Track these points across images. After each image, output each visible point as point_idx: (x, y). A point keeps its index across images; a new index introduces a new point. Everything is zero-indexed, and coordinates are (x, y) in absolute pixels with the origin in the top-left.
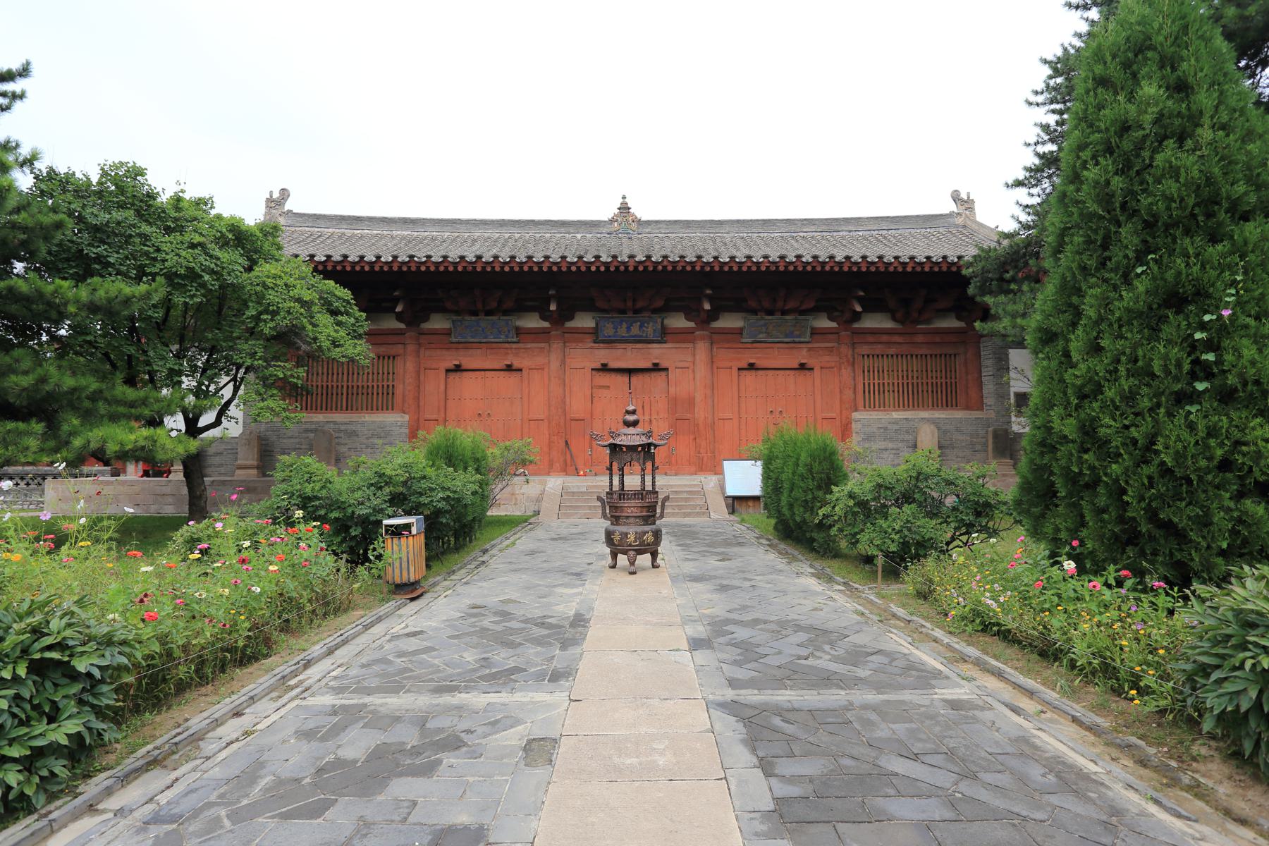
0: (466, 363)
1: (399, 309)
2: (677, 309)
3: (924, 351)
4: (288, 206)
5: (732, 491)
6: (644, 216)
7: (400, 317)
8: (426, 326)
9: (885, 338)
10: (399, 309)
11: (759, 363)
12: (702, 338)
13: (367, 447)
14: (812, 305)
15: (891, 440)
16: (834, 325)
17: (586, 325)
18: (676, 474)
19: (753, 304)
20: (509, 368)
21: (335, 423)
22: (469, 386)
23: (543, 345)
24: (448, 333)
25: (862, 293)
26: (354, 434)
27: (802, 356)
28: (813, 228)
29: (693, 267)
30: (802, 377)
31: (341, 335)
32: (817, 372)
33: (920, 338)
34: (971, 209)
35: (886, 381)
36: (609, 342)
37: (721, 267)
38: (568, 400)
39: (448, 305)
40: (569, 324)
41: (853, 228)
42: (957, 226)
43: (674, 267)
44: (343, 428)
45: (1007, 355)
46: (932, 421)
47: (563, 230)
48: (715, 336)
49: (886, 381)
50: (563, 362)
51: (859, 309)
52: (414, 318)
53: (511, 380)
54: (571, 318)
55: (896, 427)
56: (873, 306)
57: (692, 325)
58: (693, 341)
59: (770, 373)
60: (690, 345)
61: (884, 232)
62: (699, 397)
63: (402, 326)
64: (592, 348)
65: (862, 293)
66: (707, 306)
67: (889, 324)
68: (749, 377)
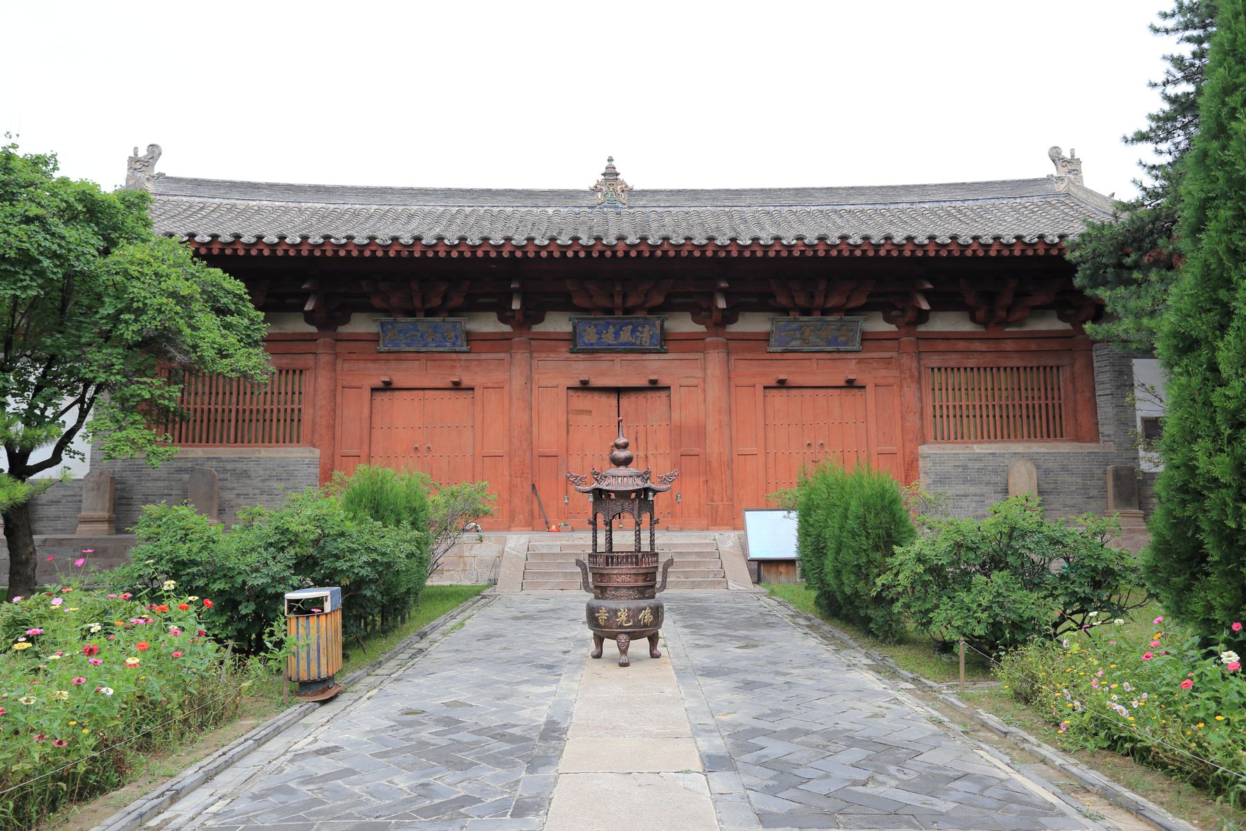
1: (309, 306)
2: (682, 308)
3: (1015, 362)
4: (159, 168)
5: (757, 552)
6: (638, 186)
7: (309, 318)
8: (344, 329)
9: (961, 345)
10: (309, 306)
11: (792, 380)
12: (716, 346)
15: (973, 482)
16: (893, 328)
17: (559, 330)
18: (681, 530)
19: (783, 300)
20: (456, 386)
21: (219, 460)
22: (402, 412)
23: (502, 355)
24: (375, 339)
25: (929, 286)
26: (245, 474)
27: (849, 369)
28: (863, 199)
29: (703, 252)
30: (849, 397)
31: (230, 340)
33: (1009, 346)
34: (1077, 172)
35: (964, 404)
36: (591, 351)
37: (740, 252)
38: (535, 430)
39: (376, 302)
40: (537, 328)
41: (916, 199)
42: (1057, 194)
43: (678, 252)
44: (229, 466)
45: (1130, 367)
46: (1030, 458)
47: (529, 202)
48: (732, 344)
49: (964, 404)
50: (529, 380)
51: (925, 306)
53: (459, 402)
54: (540, 320)
55: (981, 465)
56: (944, 302)
57: (701, 328)
58: (703, 351)
60: (699, 356)
61: (958, 204)
62: (711, 428)
63: (313, 329)
64: (567, 360)
65: (929, 286)
66: (722, 304)
67: (967, 327)
68: (779, 397)
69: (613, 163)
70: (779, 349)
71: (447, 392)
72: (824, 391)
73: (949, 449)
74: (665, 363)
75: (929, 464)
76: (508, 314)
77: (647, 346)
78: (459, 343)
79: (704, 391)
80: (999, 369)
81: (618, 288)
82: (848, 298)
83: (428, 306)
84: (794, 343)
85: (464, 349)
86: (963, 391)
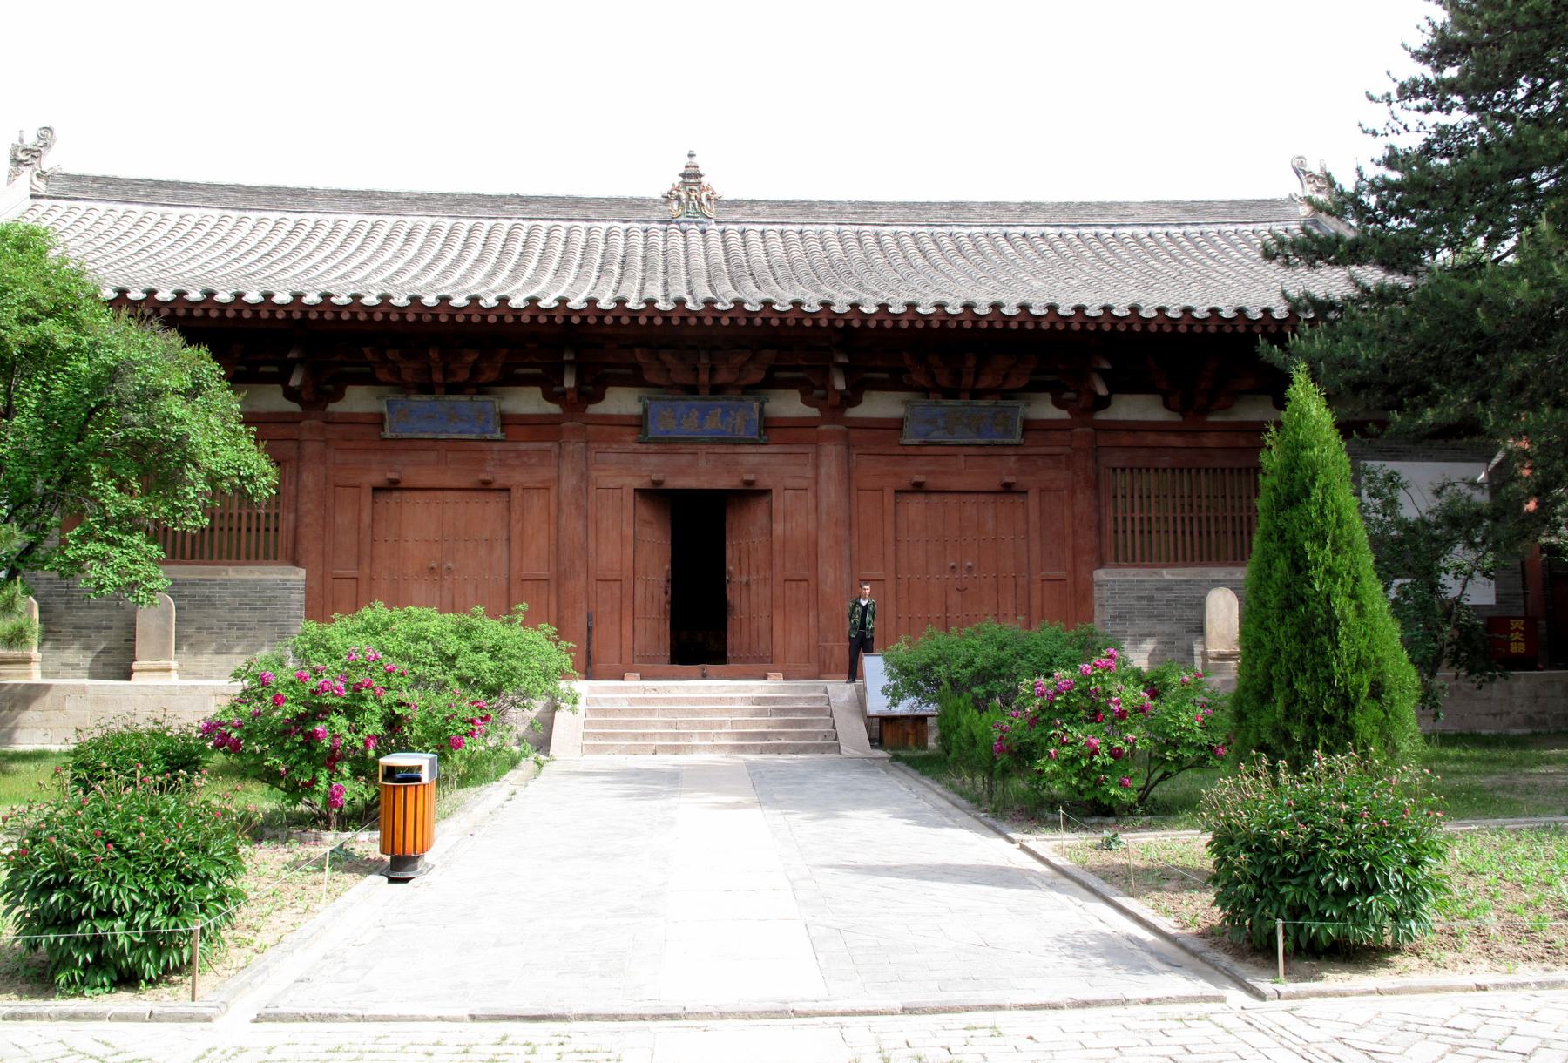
0: (413, 474)
2: (788, 385)
7: (290, 394)
9: (1151, 439)
10: (295, 381)
11: (932, 482)
13: (231, 626)
14: (1023, 383)
15: (1160, 618)
16: (1063, 414)
17: (624, 412)
20: (486, 487)
23: (547, 445)
27: (1008, 469)
31: (217, 433)
32: (1033, 499)
33: (1210, 440)
35: (1153, 515)
36: (668, 444)
38: (592, 544)
41: (1114, 221)
47: (575, 213)
48: (855, 434)
50: (585, 477)
51: (1102, 390)
52: (317, 396)
53: (491, 507)
54: (599, 397)
56: (1124, 384)
57: (813, 412)
58: (816, 442)
59: (951, 499)
60: (810, 449)
62: (824, 543)
63: (294, 407)
64: (635, 452)
66: (840, 384)
68: (915, 507)
69: (695, 161)
70: (916, 441)
71: (474, 494)
72: (973, 498)
73: (1133, 575)
74: (765, 458)
75: (1106, 593)
76: (556, 389)
77: (742, 435)
78: (491, 428)
79: (816, 496)
80: (1198, 470)
81: (704, 360)
82: (1006, 377)
83: (450, 380)
84: (935, 433)
85: (498, 435)
86: (1153, 499)
